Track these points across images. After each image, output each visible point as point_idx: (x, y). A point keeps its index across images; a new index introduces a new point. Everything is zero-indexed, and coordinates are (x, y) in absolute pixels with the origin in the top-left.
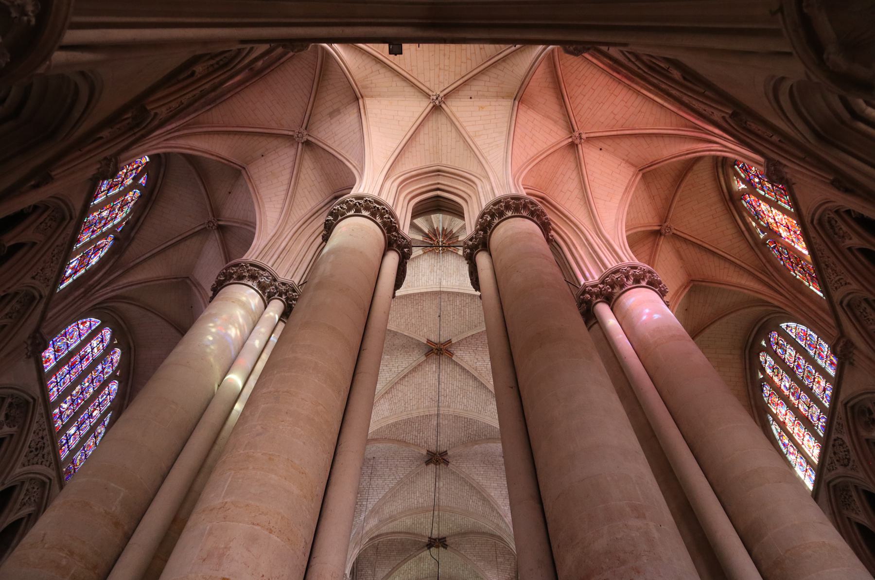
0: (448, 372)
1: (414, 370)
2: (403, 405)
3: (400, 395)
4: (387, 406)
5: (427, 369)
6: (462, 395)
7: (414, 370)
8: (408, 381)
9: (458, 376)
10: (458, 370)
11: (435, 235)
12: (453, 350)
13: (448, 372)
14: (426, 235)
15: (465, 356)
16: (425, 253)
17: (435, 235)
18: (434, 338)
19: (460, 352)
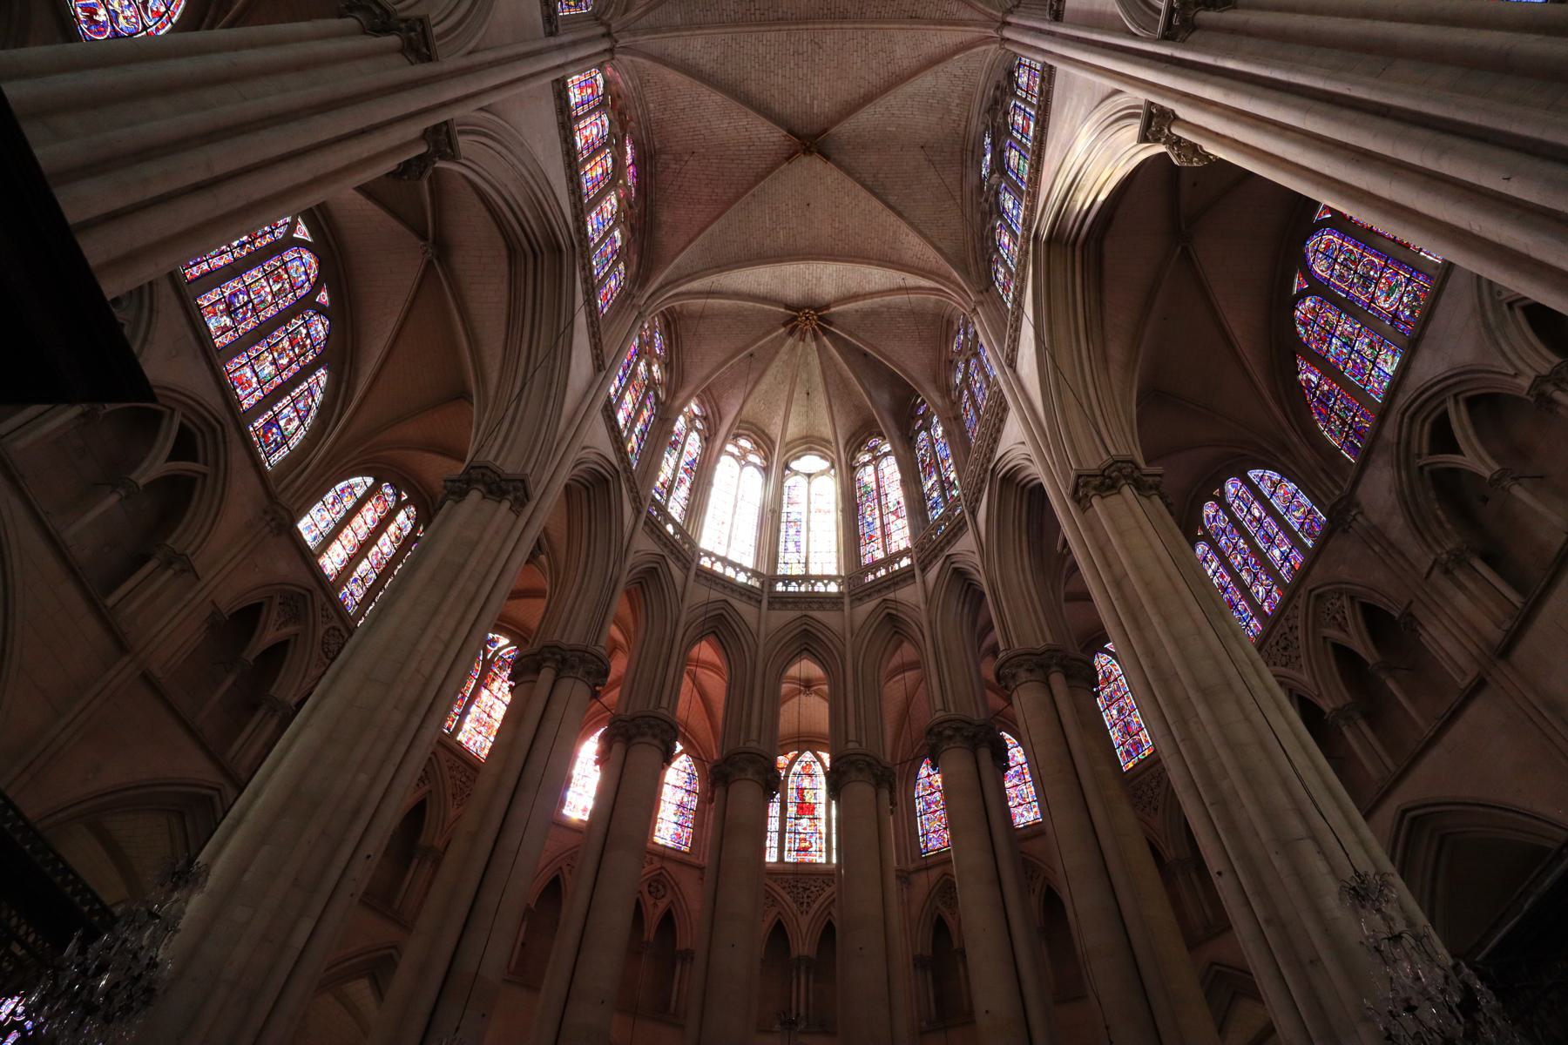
0: (792, 101)
1: (851, 108)
2: (870, 44)
3: (874, 64)
4: (900, 51)
5: (827, 104)
6: (768, 59)
7: (851, 108)
8: (860, 87)
9: (776, 95)
10: (777, 107)
11: (813, 329)
12: (786, 143)
13: (792, 101)
14: (825, 332)
15: (769, 135)
16: (828, 306)
17: (813, 329)
18: (817, 164)
19: (775, 139)
